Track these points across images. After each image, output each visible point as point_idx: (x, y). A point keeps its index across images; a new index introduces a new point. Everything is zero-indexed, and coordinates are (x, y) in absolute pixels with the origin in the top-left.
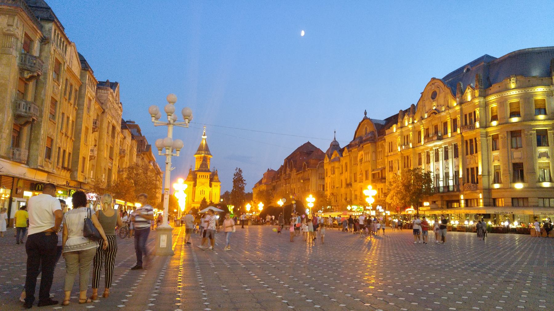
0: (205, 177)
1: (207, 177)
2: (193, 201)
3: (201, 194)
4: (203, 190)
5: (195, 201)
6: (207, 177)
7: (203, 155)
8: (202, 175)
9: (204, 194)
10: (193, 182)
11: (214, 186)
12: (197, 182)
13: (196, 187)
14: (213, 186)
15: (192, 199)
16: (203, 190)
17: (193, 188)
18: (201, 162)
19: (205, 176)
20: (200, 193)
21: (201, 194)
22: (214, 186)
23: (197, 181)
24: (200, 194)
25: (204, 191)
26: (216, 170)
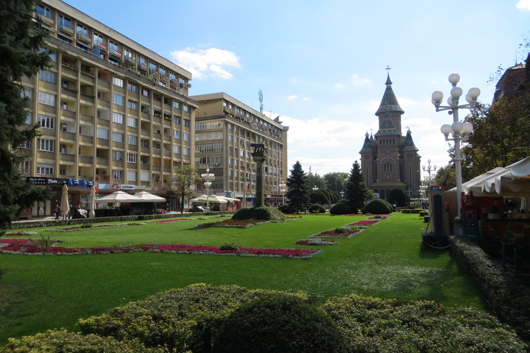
1: (394, 142)
3: (385, 170)
4: (388, 163)
6: (394, 142)
13: (377, 159)
16: (388, 163)
19: (390, 140)
20: (383, 168)
21: (385, 170)
24: (384, 170)
25: (391, 165)
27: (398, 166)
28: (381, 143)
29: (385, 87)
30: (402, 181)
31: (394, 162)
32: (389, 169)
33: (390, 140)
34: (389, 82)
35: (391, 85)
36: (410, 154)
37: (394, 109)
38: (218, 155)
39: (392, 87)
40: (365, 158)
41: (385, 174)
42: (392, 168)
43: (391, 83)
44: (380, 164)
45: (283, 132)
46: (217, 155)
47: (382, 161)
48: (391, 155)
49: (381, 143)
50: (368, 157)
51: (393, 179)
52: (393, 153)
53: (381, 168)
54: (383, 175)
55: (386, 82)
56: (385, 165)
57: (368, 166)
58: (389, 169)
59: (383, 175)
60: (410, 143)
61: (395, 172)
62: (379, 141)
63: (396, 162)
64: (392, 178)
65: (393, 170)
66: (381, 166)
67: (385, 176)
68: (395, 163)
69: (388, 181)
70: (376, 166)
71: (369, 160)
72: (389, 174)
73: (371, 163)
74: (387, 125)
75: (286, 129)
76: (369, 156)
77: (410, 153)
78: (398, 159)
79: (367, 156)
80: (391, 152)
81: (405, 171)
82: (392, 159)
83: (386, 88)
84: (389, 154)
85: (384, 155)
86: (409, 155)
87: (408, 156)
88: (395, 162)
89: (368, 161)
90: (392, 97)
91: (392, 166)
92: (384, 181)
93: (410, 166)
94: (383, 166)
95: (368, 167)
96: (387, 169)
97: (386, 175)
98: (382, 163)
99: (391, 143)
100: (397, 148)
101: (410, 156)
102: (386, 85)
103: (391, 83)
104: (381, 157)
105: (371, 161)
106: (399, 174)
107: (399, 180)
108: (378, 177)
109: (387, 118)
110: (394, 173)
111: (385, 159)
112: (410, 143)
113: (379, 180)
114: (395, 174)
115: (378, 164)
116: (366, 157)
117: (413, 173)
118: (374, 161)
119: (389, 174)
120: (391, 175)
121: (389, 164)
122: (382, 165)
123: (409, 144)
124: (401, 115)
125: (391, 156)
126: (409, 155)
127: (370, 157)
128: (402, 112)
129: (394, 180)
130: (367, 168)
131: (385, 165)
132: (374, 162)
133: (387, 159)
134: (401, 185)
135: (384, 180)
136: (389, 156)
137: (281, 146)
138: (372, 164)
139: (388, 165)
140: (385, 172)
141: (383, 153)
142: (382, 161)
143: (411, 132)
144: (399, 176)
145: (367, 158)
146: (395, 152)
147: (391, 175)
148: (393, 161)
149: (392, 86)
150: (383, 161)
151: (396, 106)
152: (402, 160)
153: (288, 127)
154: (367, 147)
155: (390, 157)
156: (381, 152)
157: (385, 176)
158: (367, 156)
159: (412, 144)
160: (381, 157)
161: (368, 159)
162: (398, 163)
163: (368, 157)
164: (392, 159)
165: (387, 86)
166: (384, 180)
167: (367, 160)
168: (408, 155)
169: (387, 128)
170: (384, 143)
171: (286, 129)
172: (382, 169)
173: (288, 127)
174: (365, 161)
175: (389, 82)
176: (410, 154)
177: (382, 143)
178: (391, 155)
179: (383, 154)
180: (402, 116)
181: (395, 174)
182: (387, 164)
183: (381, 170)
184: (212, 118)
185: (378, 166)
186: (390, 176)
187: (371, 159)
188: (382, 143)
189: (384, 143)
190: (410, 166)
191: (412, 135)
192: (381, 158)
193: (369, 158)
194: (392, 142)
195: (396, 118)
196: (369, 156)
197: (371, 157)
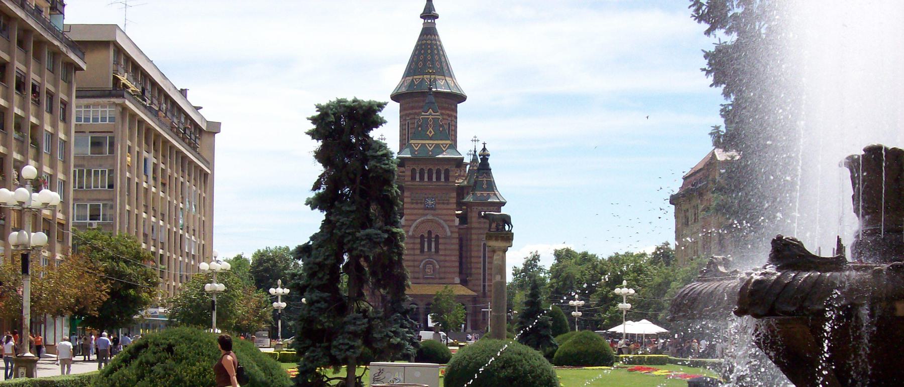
0: (438, 178)
1: (447, 178)
3: (422, 251)
4: (430, 232)
6: (447, 178)
16: (430, 232)
20: (418, 246)
21: (422, 251)
24: (418, 252)
26: (484, 149)
27: (456, 241)
28: (413, 178)
29: (419, 25)
30: (464, 282)
31: (445, 231)
32: (433, 250)
33: (438, 173)
34: (429, 14)
35: (436, 20)
37: (441, 86)
38: (99, 200)
39: (437, 27)
41: (422, 261)
43: (436, 17)
45: (205, 138)
46: (94, 200)
47: (414, 225)
48: (439, 212)
49: (413, 178)
51: (442, 276)
52: (445, 206)
54: (416, 263)
55: (422, 11)
56: (422, 237)
58: (433, 250)
59: (416, 263)
60: (485, 182)
61: (447, 258)
62: (409, 173)
63: (452, 232)
65: (441, 253)
68: (449, 234)
69: (428, 281)
72: (431, 263)
74: (431, 132)
75: (214, 129)
80: (439, 203)
81: (471, 257)
82: (442, 222)
83: (423, 29)
84: (432, 209)
85: (421, 211)
88: (448, 230)
90: (438, 54)
91: (441, 241)
92: (418, 281)
94: (418, 241)
96: (426, 249)
97: (424, 267)
98: (414, 231)
99: (438, 178)
100: (454, 195)
102: (422, 20)
103: (436, 17)
104: (412, 214)
106: (457, 264)
107: (457, 280)
109: (430, 110)
110: (446, 261)
111: (423, 222)
112: (485, 182)
114: (447, 264)
119: (431, 263)
120: (437, 267)
121: (433, 236)
122: (413, 237)
123: (485, 186)
124: (458, 105)
125: (437, 215)
128: (462, 98)
129: (444, 278)
131: (422, 237)
133: (428, 221)
134: (462, 293)
135: (418, 278)
136: (433, 215)
137: (206, 174)
139: (429, 239)
140: (421, 258)
141: (420, 206)
142: (414, 225)
143: (488, 155)
144: (458, 270)
146: (448, 204)
147: (437, 267)
148: (443, 227)
149: (440, 25)
150: (417, 227)
151: (447, 79)
153: (220, 124)
155: (435, 218)
156: (412, 203)
159: (491, 186)
160: (412, 214)
162: (456, 235)
164: (442, 222)
165: (424, 23)
166: (418, 278)
169: (431, 139)
170: (422, 178)
171: (214, 129)
172: (414, 249)
173: (220, 124)
175: (429, 14)
177: (418, 179)
178: (439, 212)
179: (422, 209)
180: (460, 106)
181: (447, 264)
182: (426, 235)
183: (412, 252)
184: (89, 94)
186: (434, 266)
188: (418, 179)
189: (422, 178)
191: (490, 161)
192: (413, 217)
194: (443, 176)
195: (448, 112)
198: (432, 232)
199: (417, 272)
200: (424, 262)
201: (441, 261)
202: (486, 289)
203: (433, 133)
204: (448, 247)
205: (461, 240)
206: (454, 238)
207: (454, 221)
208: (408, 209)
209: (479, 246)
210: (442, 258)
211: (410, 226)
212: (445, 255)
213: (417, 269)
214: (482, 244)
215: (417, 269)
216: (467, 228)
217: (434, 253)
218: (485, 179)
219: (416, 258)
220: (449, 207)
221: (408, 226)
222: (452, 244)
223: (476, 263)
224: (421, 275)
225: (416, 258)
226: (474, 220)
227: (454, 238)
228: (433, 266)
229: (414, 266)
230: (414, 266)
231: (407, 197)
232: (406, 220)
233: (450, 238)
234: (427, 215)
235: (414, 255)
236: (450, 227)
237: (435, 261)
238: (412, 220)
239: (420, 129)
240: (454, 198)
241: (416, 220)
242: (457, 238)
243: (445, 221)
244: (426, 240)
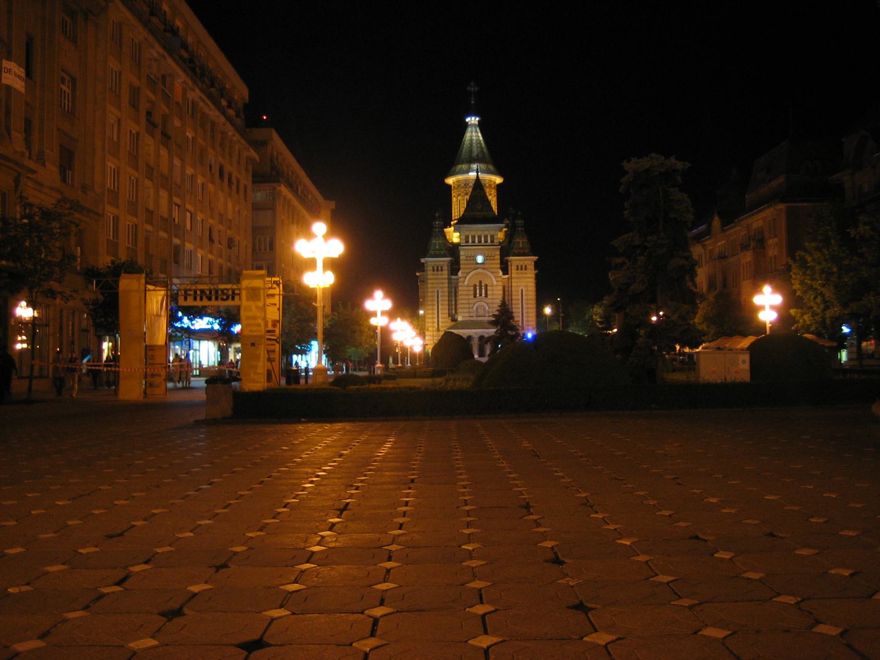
2: (454, 320)
3: (475, 296)
4: (480, 282)
5: (460, 318)
7: (473, 175)
8: (477, 234)
9: (486, 296)
10: (448, 259)
11: (514, 268)
12: (461, 258)
13: (460, 274)
14: (513, 269)
15: (450, 315)
16: (480, 282)
17: (449, 279)
18: (468, 197)
20: (472, 293)
21: (475, 296)
22: (514, 268)
23: (462, 253)
24: (472, 297)
25: (486, 286)
27: (501, 288)
31: (492, 280)
32: (483, 295)
36: (522, 266)
40: (433, 270)
41: (475, 304)
42: (489, 292)
44: (466, 283)
50: (440, 268)
53: (466, 293)
54: (471, 306)
57: (440, 288)
58: (483, 295)
60: (521, 243)
63: (497, 281)
64: (489, 312)
65: (489, 297)
66: (467, 288)
67: (475, 308)
68: (495, 283)
70: (456, 288)
71: (442, 275)
73: (447, 281)
76: (442, 268)
77: (521, 262)
78: (501, 273)
79: (438, 267)
85: (473, 266)
86: (519, 267)
87: (517, 269)
88: (494, 280)
89: (440, 277)
93: (522, 290)
94: (472, 288)
95: (439, 291)
96: (478, 295)
97: (477, 309)
98: (469, 281)
101: (522, 269)
105: (447, 277)
108: (459, 311)
110: (492, 303)
111: (475, 274)
112: (521, 243)
113: (463, 317)
115: (460, 284)
116: (436, 268)
117: (527, 304)
118: (453, 277)
120: (487, 308)
121: (483, 284)
122: (468, 286)
126: (519, 267)
127: (443, 269)
130: (438, 291)
131: (475, 286)
132: (451, 279)
133: (479, 273)
136: (483, 269)
138: (448, 283)
140: (474, 301)
141: (472, 262)
145: (438, 270)
146: (494, 260)
150: (470, 278)
152: (507, 276)
154: (437, 247)
155: (484, 271)
156: (467, 260)
157: (475, 308)
158: (438, 267)
161: (440, 272)
162: (500, 283)
163: (440, 268)
167: (438, 275)
168: (517, 267)
174: (435, 277)
176: (522, 266)
182: (478, 284)
185: (460, 288)
187: (446, 272)
190: (522, 290)
192: (467, 271)
193: (442, 270)
196: (442, 268)
197: (445, 268)
198: (483, 281)
199: (471, 312)
200: (476, 304)
201: (489, 303)
202: (524, 324)
203: (481, 206)
204: (495, 292)
205: (504, 288)
206: (499, 286)
207: (499, 272)
208: (464, 264)
209: (518, 291)
210: (491, 301)
211: (466, 278)
212: (493, 299)
213: (471, 310)
214: (520, 290)
215: (471, 310)
216: (508, 278)
217: (483, 298)
218: (520, 240)
219: (471, 301)
220: (494, 262)
221: (463, 277)
222: (498, 290)
223: (516, 304)
224: (474, 315)
225: (471, 301)
226: (513, 271)
227: (499, 286)
228: (484, 308)
229: (469, 308)
230: (469, 308)
231: (463, 256)
232: (462, 273)
233: (497, 286)
234: (477, 269)
235: (469, 299)
236: (495, 277)
237: (485, 304)
238: (467, 273)
239: (471, 204)
240: (498, 255)
241: (468, 273)
242: (501, 286)
243: (492, 273)
244: (478, 288)
